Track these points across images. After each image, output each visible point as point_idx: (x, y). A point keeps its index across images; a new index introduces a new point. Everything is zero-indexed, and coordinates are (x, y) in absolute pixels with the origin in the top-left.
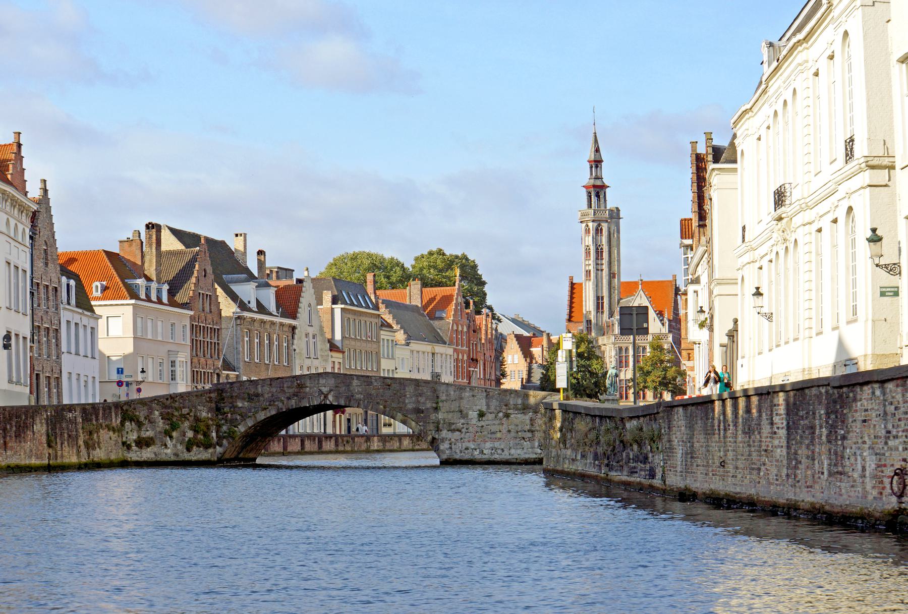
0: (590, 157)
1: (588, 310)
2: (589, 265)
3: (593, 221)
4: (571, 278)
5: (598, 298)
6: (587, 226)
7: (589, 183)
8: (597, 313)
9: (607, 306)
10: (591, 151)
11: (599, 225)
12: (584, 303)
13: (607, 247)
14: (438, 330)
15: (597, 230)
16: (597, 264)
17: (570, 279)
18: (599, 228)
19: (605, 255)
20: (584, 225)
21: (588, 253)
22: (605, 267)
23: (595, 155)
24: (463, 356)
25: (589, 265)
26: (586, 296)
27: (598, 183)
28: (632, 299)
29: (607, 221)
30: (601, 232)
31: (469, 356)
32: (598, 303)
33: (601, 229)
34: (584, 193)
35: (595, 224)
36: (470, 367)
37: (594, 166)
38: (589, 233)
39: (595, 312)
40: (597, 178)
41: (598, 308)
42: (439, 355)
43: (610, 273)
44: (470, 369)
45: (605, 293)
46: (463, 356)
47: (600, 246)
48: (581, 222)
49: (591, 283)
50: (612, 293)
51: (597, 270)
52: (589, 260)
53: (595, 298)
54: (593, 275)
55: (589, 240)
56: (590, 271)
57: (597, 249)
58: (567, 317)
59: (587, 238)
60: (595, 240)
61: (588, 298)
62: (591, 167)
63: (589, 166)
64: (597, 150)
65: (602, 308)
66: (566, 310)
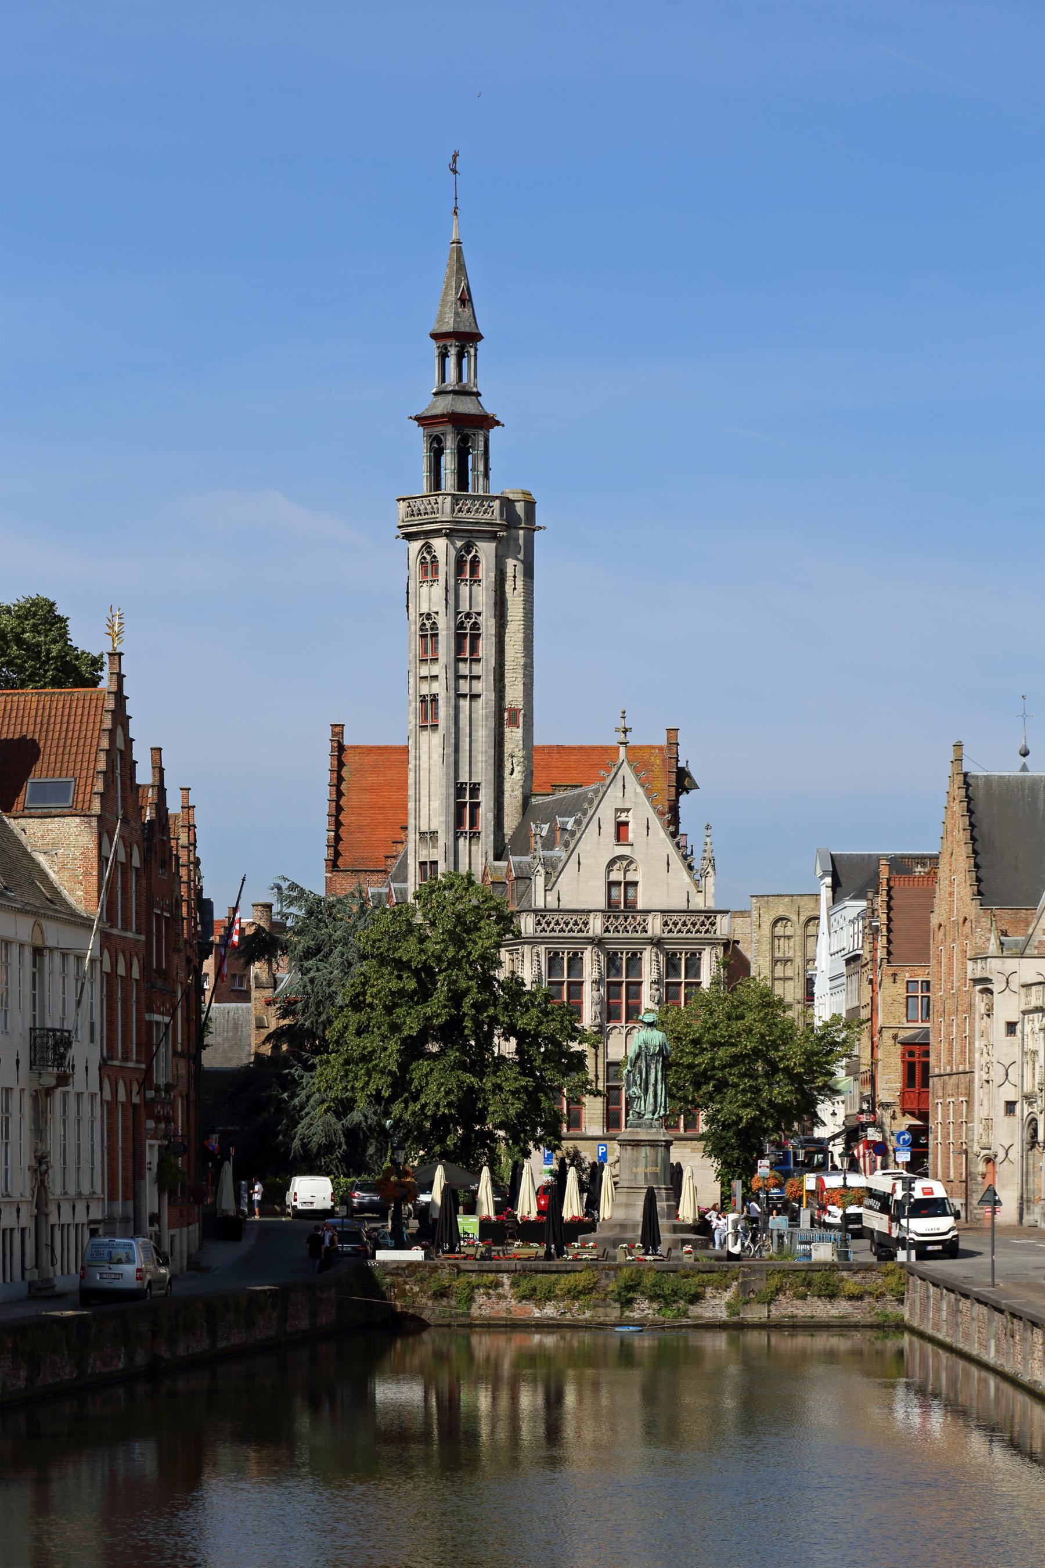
0: (441, 319)
1: (424, 828)
2: (435, 677)
3: (450, 534)
4: (338, 730)
5: (459, 789)
6: (428, 547)
7: (433, 406)
8: (456, 839)
9: (491, 816)
10: (444, 301)
12: (411, 805)
13: (492, 622)
14: (41, 859)
16: (458, 677)
19: (486, 648)
20: (416, 545)
21: (428, 634)
22: (484, 687)
23: (457, 314)
24: (129, 967)
27: (465, 406)
28: (596, 792)
29: (492, 536)
30: (474, 571)
31: (145, 968)
32: (459, 807)
33: (475, 563)
34: (418, 439)
36: (150, 1010)
37: (453, 351)
38: (436, 572)
39: (452, 833)
40: (463, 392)
41: (459, 822)
42: (57, 958)
44: (147, 1017)
45: (483, 775)
46: (129, 967)
47: (468, 615)
48: (409, 537)
49: (437, 738)
50: (507, 771)
51: (459, 696)
53: (452, 791)
54: (444, 711)
56: (434, 698)
57: (460, 626)
58: (324, 853)
59: (425, 588)
60: (453, 596)
61: (424, 792)
62: (443, 356)
63: (436, 352)
64: (465, 300)
65: (473, 822)
66: (323, 833)
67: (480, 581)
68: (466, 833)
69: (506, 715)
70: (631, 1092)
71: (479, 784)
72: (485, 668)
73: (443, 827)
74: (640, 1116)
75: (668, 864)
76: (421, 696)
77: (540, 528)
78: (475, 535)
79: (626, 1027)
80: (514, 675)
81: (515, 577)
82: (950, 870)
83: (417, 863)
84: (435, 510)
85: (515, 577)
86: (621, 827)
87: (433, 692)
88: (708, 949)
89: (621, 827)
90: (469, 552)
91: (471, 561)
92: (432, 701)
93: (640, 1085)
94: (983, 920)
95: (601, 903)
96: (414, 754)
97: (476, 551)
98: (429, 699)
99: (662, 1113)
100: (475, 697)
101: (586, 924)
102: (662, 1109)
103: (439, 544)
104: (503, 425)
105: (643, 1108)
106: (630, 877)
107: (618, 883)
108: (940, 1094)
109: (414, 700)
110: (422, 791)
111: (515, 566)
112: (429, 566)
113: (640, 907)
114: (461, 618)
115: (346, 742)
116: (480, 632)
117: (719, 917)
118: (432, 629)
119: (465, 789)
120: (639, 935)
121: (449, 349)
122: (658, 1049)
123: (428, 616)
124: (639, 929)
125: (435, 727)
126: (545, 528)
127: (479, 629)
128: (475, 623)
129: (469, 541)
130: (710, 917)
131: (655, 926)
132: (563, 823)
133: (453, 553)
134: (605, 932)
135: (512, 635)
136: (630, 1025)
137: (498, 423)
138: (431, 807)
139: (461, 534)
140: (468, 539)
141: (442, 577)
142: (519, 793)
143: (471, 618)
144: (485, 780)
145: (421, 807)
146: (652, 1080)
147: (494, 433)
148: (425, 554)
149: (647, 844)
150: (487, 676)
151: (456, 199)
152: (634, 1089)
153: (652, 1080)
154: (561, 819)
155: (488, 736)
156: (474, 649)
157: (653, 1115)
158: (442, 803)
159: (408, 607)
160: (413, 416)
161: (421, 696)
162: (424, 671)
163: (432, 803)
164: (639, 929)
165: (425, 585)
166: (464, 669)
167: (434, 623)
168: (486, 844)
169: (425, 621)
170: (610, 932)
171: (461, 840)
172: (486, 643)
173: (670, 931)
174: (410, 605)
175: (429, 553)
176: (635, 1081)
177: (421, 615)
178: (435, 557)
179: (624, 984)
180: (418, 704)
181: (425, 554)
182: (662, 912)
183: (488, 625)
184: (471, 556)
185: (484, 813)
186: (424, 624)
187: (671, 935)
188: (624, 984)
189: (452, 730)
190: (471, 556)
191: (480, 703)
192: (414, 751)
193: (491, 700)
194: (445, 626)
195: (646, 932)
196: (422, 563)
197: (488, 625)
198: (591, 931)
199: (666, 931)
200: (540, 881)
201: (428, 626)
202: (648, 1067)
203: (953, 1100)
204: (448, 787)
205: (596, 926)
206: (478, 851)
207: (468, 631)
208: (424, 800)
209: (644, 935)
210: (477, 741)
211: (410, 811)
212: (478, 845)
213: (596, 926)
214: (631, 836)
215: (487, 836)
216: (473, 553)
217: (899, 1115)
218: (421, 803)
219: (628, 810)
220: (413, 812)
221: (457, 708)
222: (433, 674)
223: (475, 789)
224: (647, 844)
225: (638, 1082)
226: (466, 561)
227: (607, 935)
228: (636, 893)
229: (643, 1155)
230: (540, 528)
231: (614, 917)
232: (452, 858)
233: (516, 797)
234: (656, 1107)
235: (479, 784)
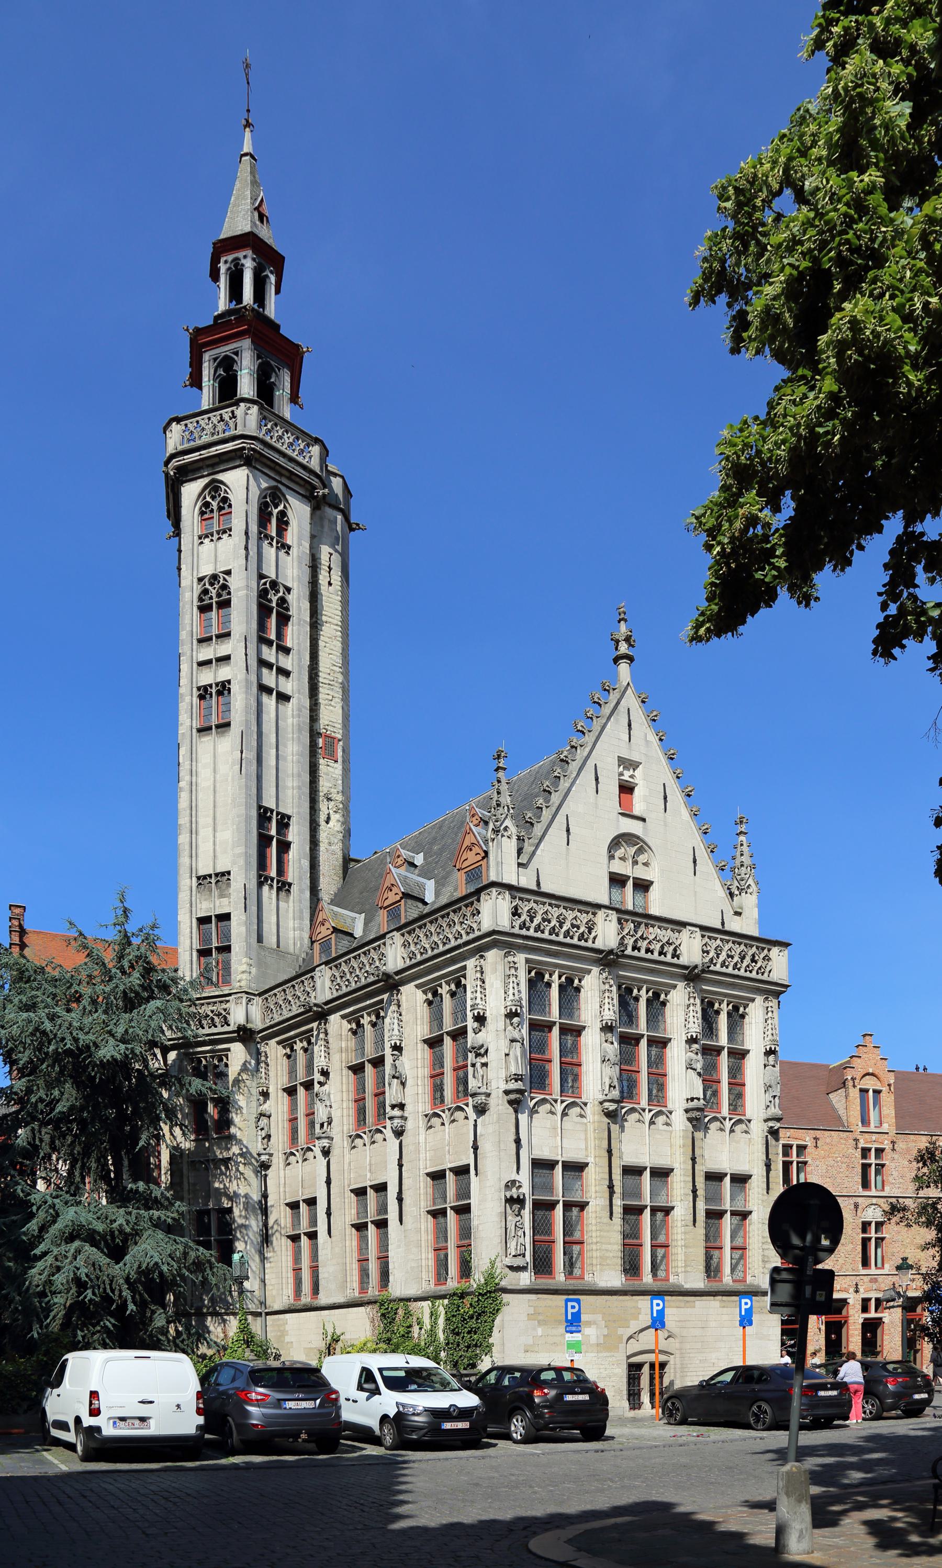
5: (264, 815)
8: (260, 885)
9: (306, 864)
12: (183, 839)
18: (275, 511)
22: (295, 686)
26: (192, 808)
32: (264, 841)
41: (262, 864)
47: (274, 584)
56: (224, 688)
61: (205, 820)
68: (272, 879)
71: (289, 817)
72: (297, 662)
73: (242, 862)
75: (695, 861)
76: (199, 689)
78: (284, 481)
83: (194, 921)
88: (759, 999)
92: (220, 693)
96: (188, 767)
97: (285, 507)
98: (214, 691)
100: (283, 698)
109: (189, 692)
110: (201, 821)
114: (265, 584)
116: (290, 613)
117: (775, 951)
119: (270, 819)
129: (276, 488)
130: (763, 949)
133: (255, 493)
138: (218, 840)
140: (274, 483)
142: (337, 848)
144: (299, 813)
145: (200, 843)
149: (665, 825)
150: (300, 673)
155: (300, 754)
158: (238, 829)
159: (179, 569)
161: (199, 689)
163: (218, 834)
165: (207, 541)
167: (224, 587)
168: (300, 901)
171: (266, 888)
172: (299, 630)
174: (183, 567)
177: (200, 580)
178: (225, 500)
180: (195, 700)
181: (208, 499)
183: (299, 605)
185: (296, 857)
189: (254, 728)
191: (289, 709)
192: (189, 762)
193: (305, 708)
197: (299, 605)
204: (248, 806)
206: (287, 911)
208: (205, 833)
210: (285, 759)
211: (181, 847)
212: (287, 902)
215: (301, 891)
216: (281, 507)
218: (200, 837)
220: (187, 847)
221: (259, 705)
223: (284, 823)
224: (665, 825)
226: (271, 514)
232: (255, 908)
233: (334, 853)
235: (289, 817)
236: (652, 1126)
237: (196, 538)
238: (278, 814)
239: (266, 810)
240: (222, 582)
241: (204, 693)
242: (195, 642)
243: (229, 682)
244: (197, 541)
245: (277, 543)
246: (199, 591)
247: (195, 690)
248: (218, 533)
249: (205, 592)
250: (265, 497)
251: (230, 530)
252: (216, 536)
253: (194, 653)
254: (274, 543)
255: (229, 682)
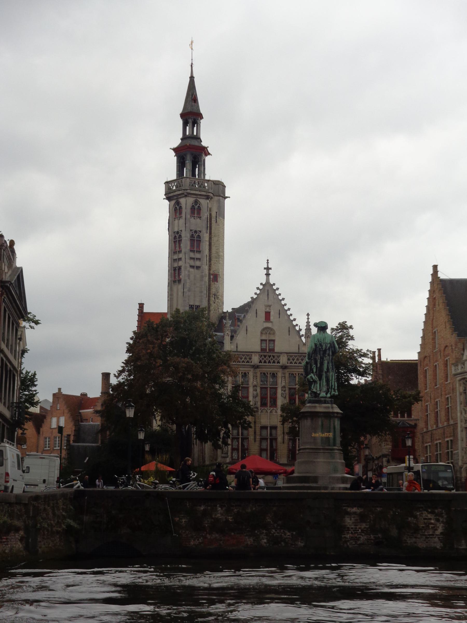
4: (141, 306)
6: (178, 203)
11: (196, 202)
15: (193, 208)
17: (140, 307)
18: (196, 207)
20: (173, 202)
25: (180, 259)
27: (195, 143)
30: (199, 213)
33: (199, 209)
35: (191, 200)
38: (180, 213)
43: (210, 274)
47: (196, 232)
50: (212, 302)
52: (180, 252)
55: (180, 224)
56: (180, 268)
57: (192, 236)
59: (176, 221)
67: (201, 217)
69: (212, 277)
70: (309, 377)
74: (316, 395)
76: (173, 268)
77: (227, 197)
78: (198, 197)
79: (270, 409)
80: (216, 259)
81: (216, 217)
82: (432, 327)
84: (181, 185)
85: (216, 217)
86: (268, 315)
87: (179, 265)
89: (268, 315)
90: (196, 205)
91: (197, 208)
93: (316, 372)
94: (459, 344)
95: (257, 348)
97: (199, 204)
98: (177, 269)
99: (333, 393)
100: (198, 268)
101: (250, 359)
102: (333, 390)
103: (183, 201)
104: (211, 155)
105: (318, 389)
106: (272, 338)
107: (266, 340)
108: (429, 440)
111: (216, 212)
112: (178, 211)
113: (276, 350)
114: (192, 233)
115: (146, 310)
118: (179, 238)
120: (276, 364)
121: (188, 120)
122: (329, 345)
123: (178, 232)
124: (276, 361)
125: (180, 281)
126: (229, 197)
127: (200, 238)
128: (199, 235)
129: (196, 200)
131: (283, 360)
132: (239, 316)
134: (259, 363)
135: (215, 242)
136: (272, 408)
137: (209, 154)
139: (192, 196)
140: (195, 199)
141: (183, 215)
143: (197, 233)
146: (325, 369)
147: (209, 156)
148: (176, 206)
151: (192, 60)
152: (312, 375)
153: (325, 369)
154: (237, 314)
156: (199, 246)
157: (326, 394)
160: (172, 148)
162: (176, 257)
164: (276, 361)
166: (192, 255)
167: (180, 235)
169: (176, 235)
170: (262, 363)
173: (291, 363)
175: (178, 205)
176: (312, 370)
177: (174, 232)
178: (181, 207)
179: (269, 388)
180: (173, 272)
181: (176, 206)
182: (287, 353)
184: (197, 206)
186: (175, 236)
187: (291, 364)
188: (269, 388)
190: (197, 206)
194: (186, 237)
195: (279, 363)
196: (175, 210)
198: (253, 362)
199: (289, 363)
200: (227, 340)
201: (177, 237)
202: (322, 359)
203: (440, 441)
205: (255, 359)
207: (195, 239)
209: (278, 364)
213: (255, 359)
214: (272, 318)
216: (198, 205)
217: (391, 461)
219: (270, 306)
222: (180, 257)
225: (315, 370)
226: (195, 208)
227: (261, 364)
228: (274, 345)
229: (320, 423)
230: (227, 197)
231: (264, 356)
234: (328, 389)
236: (271, 413)
237: (173, 219)
238: (195, 306)
239: (191, 306)
240: (180, 234)
241: (175, 269)
242: (173, 253)
243: (181, 266)
244: (173, 219)
245: (197, 217)
246: (174, 236)
247: (172, 268)
248: (179, 217)
249: (175, 236)
250: (193, 204)
251: (182, 217)
252: (178, 218)
253: (172, 256)
254: (196, 218)
255: (181, 266)
